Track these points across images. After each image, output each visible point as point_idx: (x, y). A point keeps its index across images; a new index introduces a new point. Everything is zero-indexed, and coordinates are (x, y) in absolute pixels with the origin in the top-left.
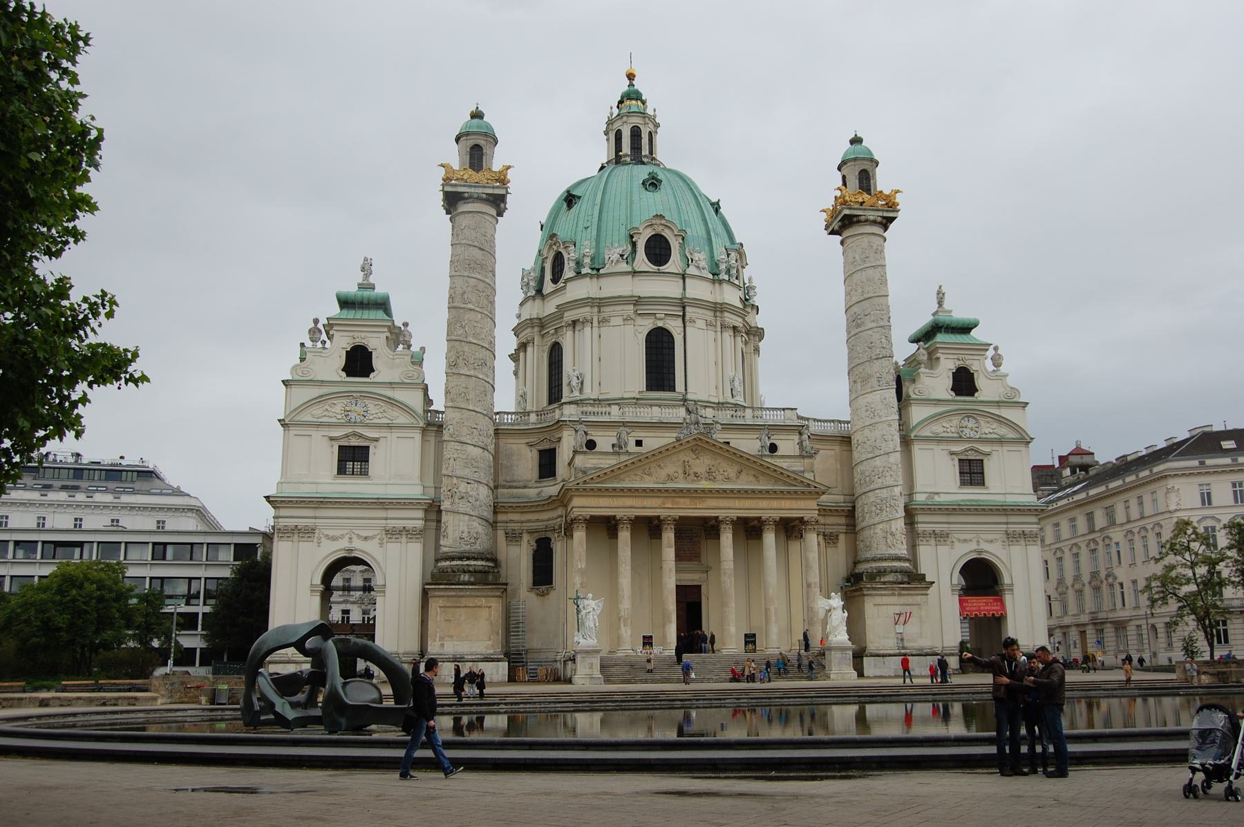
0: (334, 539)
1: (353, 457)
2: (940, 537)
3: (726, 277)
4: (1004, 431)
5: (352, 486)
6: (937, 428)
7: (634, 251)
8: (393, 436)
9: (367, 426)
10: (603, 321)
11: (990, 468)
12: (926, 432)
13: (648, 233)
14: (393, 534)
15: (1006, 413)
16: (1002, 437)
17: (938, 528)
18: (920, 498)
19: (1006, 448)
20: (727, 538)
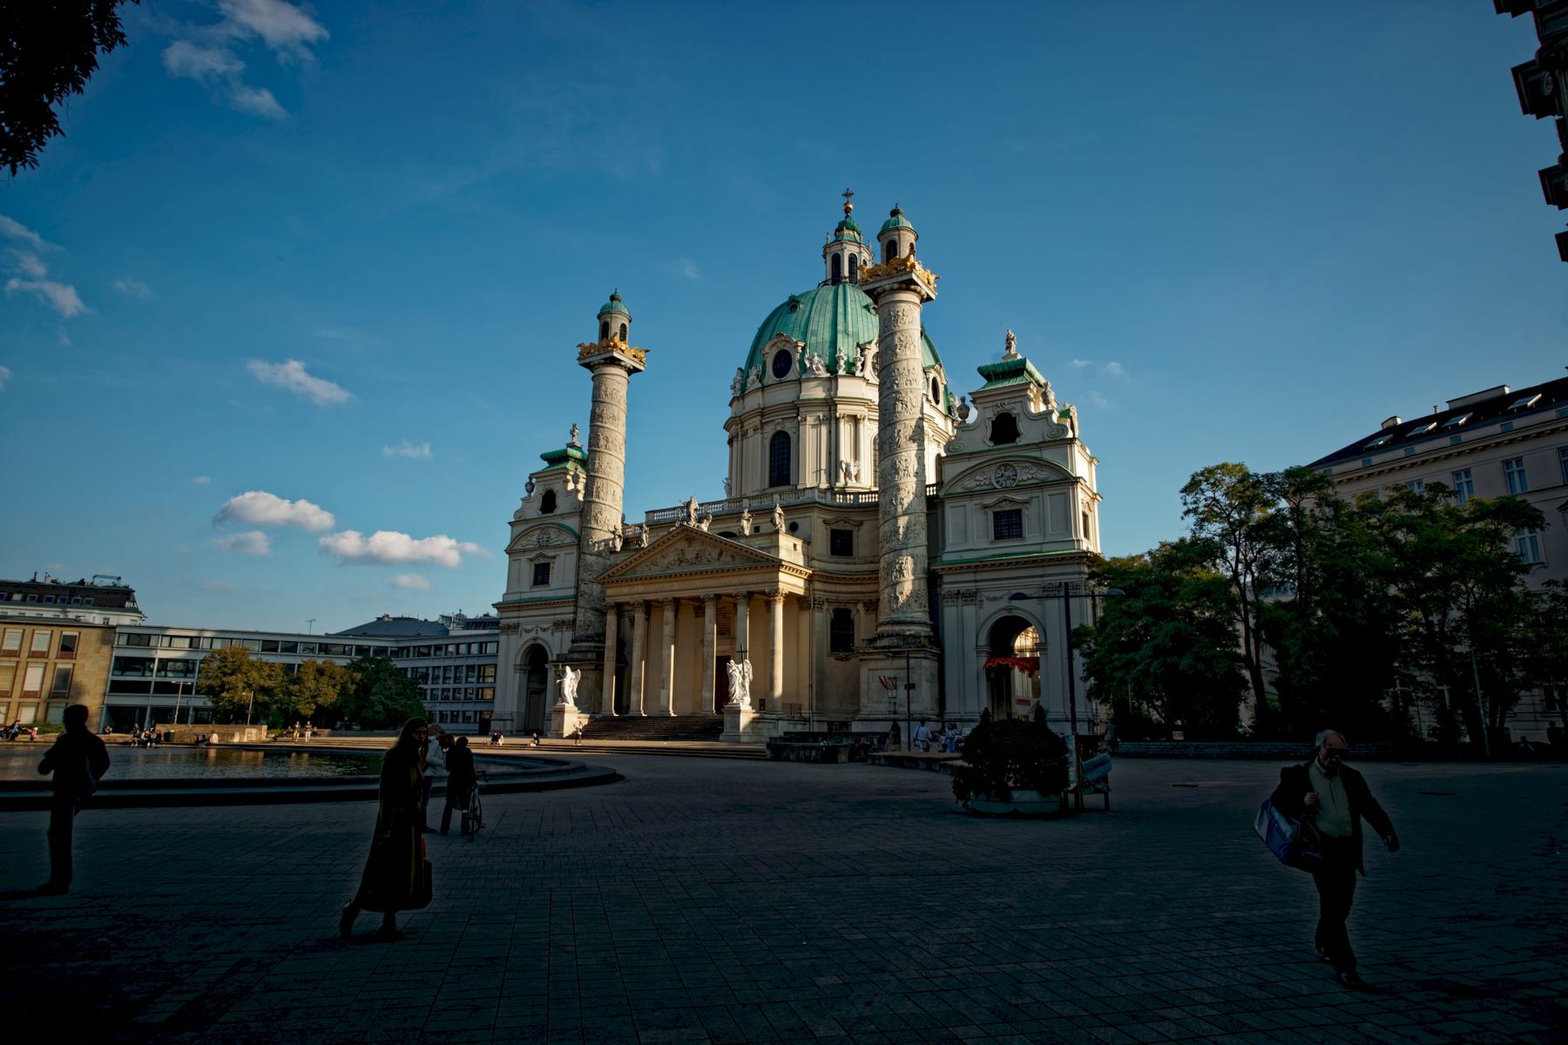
0: (528, 631)
1: (542, 574)
2: (970, 596)
3: (841, 372)
4: (1043, 474)
5: (541, 593)
6: (970, 484)
7: (764, 371)
8: (561, 553)
9: (547, 547)
10: (744, 434)
11: (1029, 517)
12: (960, 490)
13: (774, 351)
14: (559, 625)
15: (1049, 455)
16: (1044, 481)
17: (963, 587)
18: (946, 558)
19: (1046, 494)
20: (710, 612)
